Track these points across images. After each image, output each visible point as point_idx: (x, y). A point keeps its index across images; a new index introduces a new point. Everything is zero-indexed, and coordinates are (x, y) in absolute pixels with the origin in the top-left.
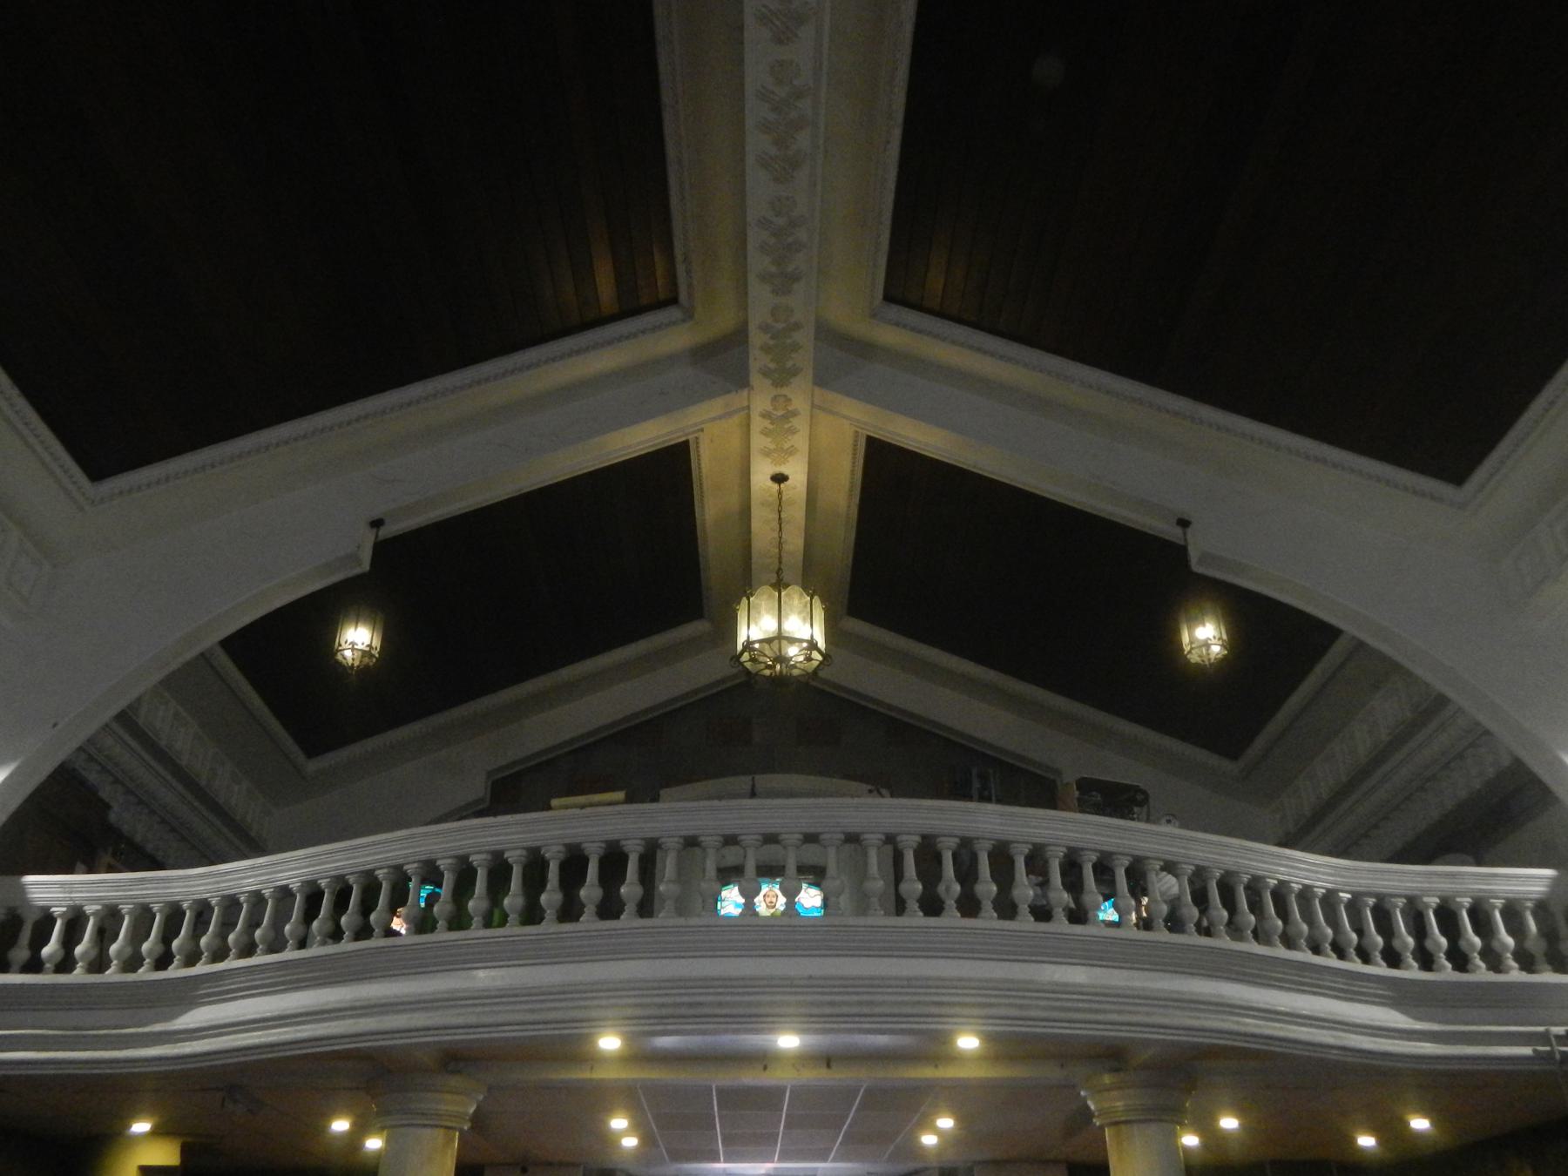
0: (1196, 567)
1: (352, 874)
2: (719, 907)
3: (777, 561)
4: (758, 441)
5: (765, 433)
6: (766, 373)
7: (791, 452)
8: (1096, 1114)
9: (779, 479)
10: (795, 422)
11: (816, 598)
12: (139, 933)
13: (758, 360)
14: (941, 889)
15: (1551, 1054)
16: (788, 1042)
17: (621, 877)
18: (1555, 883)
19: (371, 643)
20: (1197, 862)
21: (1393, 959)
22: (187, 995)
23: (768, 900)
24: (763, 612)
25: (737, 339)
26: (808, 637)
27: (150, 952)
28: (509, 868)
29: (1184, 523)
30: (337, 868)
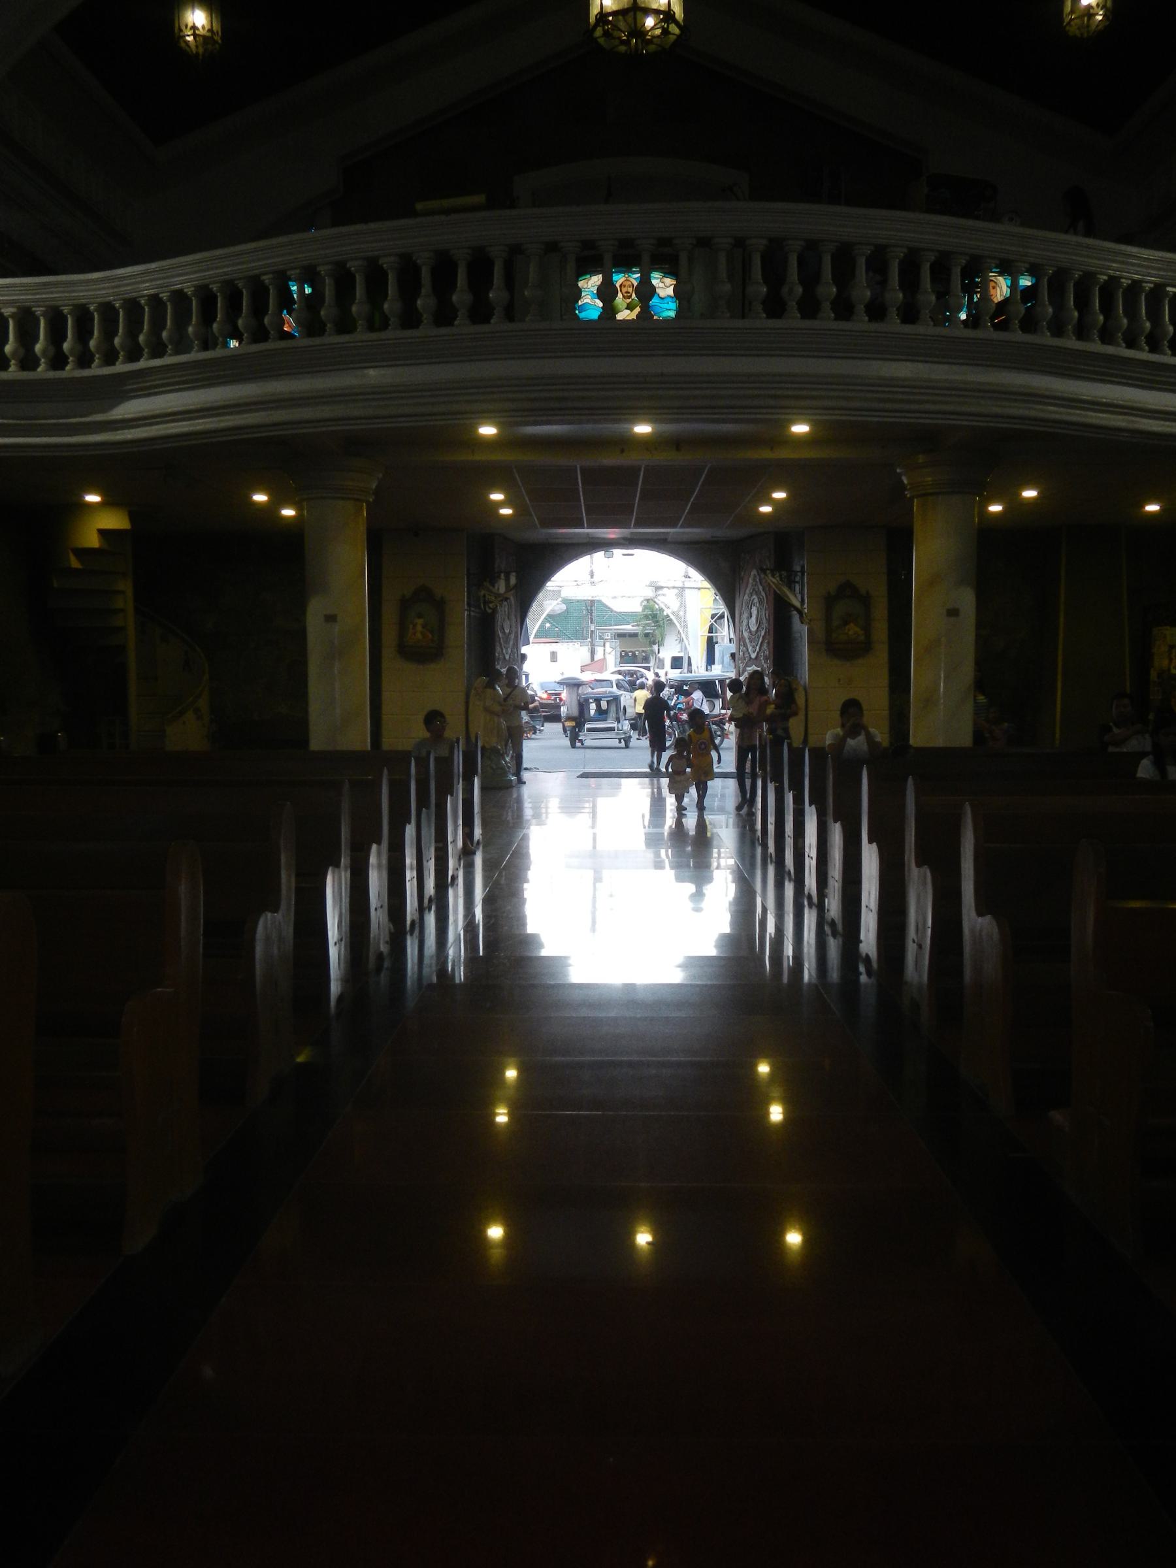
1: (240, 279)
8: (908, 487)
14: (785, 290)
16: (643, 429)
19: (212, 26)
20: (1032, 260)
22: (118, 389)
23: (624, 290)
27: (72, 350)
28: (384, 274)
30: (225, 274)
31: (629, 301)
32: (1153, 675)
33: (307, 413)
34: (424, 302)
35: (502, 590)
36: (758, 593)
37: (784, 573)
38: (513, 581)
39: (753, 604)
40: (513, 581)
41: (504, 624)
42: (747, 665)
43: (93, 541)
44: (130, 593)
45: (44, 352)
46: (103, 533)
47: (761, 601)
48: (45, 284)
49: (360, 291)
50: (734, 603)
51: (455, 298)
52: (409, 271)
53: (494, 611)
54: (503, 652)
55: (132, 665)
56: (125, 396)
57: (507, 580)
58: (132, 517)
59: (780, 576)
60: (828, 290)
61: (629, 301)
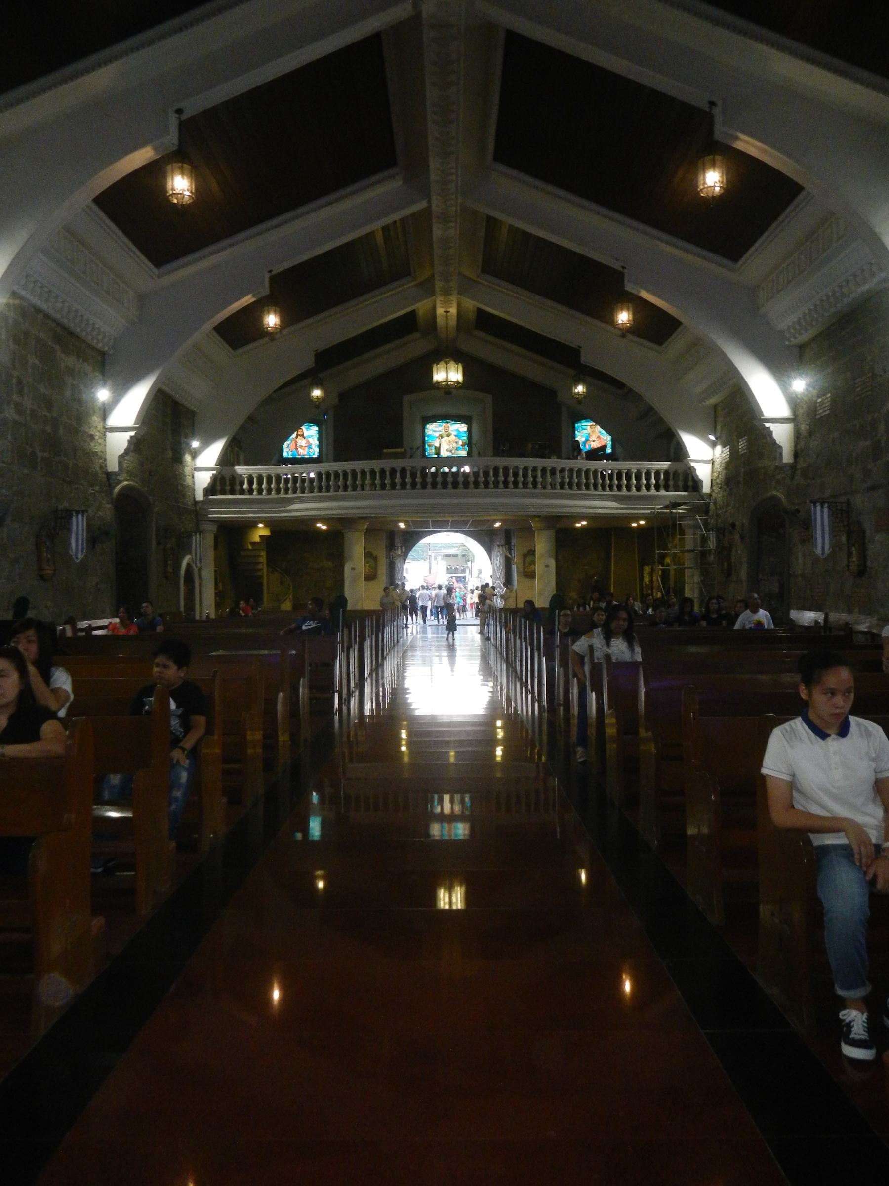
0: (582, 362)
3: (445, 319)
4: (438, 305)
6: (441, 295)
7: (451, 307)
9: (447, 312)
10: (452, 302)
11: (460, 364)
13: (437, 290)
15: (654, 513)
21: (619, 488)
22: (291, 501)
23: (445, 429)
24: (441, 371)
25: (431, 278)
26: (455, 380)
29: (580, 347)
31: (447, 433)
32: (644, 585)
35: (399, 553)
36: (499, 552)
37: (507, 546)
38: (404, 550)
39: (498, 556)
40: (404, 550)
41: (398, 564)
43: (257, 539)
44: (265, 557)
46: (260, 536)
47: (500, 555)
48: (267, 469)
49: (368, 477)
51: (396, 480)
52: (383, 472)
54: (398, 576)
55: (265, 584)
57: (401, 549)
58: (272, 531)
59: (505, 547)
60: (501, 478)
61: (447, 433)
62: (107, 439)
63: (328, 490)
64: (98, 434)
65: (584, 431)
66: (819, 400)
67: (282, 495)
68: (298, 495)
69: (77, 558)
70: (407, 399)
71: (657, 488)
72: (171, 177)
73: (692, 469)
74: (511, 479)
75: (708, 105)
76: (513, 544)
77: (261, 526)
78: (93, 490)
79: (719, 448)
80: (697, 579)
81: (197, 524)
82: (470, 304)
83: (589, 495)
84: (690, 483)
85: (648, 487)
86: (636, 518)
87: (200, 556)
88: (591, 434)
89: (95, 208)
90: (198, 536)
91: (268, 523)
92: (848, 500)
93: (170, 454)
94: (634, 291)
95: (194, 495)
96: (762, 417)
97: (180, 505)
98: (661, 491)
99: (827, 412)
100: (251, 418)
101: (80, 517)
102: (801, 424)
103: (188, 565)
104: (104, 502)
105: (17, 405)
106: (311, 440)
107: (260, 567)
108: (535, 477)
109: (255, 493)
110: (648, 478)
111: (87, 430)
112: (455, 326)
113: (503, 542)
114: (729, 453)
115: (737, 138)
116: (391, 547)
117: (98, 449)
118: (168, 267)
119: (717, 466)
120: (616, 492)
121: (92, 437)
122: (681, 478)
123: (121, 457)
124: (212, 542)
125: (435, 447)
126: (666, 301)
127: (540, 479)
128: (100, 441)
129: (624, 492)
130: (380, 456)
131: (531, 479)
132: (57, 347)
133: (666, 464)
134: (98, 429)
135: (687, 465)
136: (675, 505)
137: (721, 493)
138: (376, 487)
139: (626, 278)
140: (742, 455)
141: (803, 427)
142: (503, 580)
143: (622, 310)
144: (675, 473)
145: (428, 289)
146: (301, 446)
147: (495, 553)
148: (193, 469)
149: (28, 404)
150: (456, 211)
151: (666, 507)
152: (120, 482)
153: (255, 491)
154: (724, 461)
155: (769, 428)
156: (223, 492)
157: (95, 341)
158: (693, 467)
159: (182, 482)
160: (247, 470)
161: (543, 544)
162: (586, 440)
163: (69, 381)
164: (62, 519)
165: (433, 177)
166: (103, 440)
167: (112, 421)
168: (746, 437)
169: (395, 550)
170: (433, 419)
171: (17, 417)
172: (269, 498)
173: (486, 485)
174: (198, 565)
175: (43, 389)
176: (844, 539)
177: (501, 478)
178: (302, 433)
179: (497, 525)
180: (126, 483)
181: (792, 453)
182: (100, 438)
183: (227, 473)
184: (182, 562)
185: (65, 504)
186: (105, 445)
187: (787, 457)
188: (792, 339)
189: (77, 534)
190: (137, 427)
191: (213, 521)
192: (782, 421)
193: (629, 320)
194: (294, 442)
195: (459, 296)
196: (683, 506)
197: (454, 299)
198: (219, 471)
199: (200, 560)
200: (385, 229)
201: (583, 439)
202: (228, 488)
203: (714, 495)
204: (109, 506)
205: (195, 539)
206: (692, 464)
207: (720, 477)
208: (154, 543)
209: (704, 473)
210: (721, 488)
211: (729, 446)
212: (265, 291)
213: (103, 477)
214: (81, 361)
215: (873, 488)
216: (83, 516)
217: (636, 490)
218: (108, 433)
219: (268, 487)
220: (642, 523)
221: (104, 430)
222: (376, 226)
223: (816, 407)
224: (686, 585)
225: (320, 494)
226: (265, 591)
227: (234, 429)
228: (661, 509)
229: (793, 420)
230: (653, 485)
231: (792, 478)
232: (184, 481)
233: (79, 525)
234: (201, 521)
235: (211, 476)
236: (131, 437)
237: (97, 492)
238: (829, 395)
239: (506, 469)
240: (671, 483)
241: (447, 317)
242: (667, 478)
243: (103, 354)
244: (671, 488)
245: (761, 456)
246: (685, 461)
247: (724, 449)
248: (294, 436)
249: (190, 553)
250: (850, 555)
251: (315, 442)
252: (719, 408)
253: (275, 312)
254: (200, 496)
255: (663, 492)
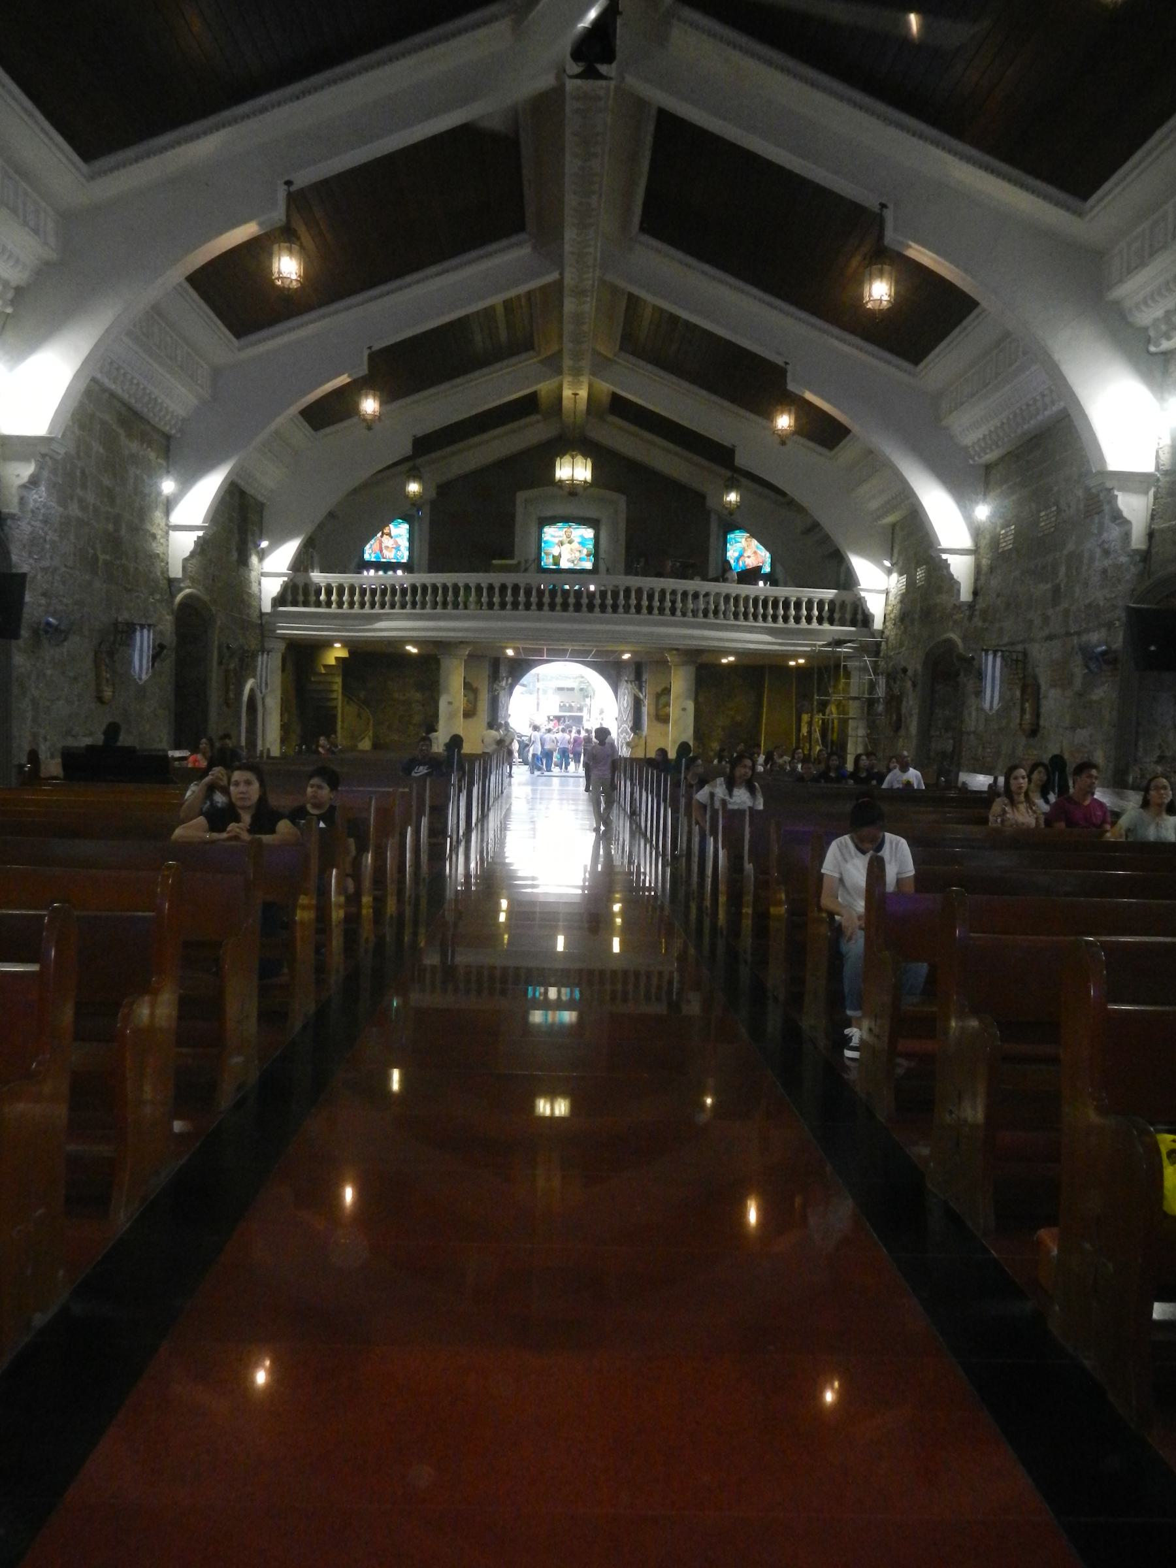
0: (736, 464)
2: (543, 536)
5: (569, 385)
6: (570, 374)
7: (581, 389)
9: (576, 394)
11: (589, 460)
12: (352, 594)
13: (565, 369)
17: (518, 595)
18: (836, 594)
21: (775, 618)
22: (378, 618)
26: (582, 479)
28: (482, 589)
29: (734, 446)
31: (569, 539)
33: (452, 634)
34: (496, 599)
36: (627, 689)
37: (637, 682)
40: (510, 681)
42: (622, 724)
43: (332, 662)
44: (340, 684)
45: (347, 600)
46: (337, 658)
47: (629, 693)
50: (617, 693)
53: (498, 694)
54: (501, 713)
56: (381, 620)
58: (350, 652)
60: (633, 601)
61: (569, 539)
62: (170, 539)
63: (423, 607)
64: (160, 532)
65: (738, 544)
66: (1003, 532)
67: (367, 610)
68: (387, 610)
69: (140, 679)
70: (521, 496)
71: (820, 620)
72: (277, 258)
73: (862, 600)
74: (645, 603)
75: (879, 207)
76: (644, 680)
77: (337, 645)
78: (153, 599)
79: (895, 576)
80: (861, 732)
81: (262, 642)
82: (605, 387)
83: (739, 626)
84: (860, 617)
85: (809, 619)
86: (795, 656)
87: (266, 678)
88: (746, 548)
89: (187, 285)
90: (265, 656)
91: (346, 643)
92: (1025, 649)
93: (235, 556)
94: (797, 392)
95: (260, 605)
96: (939, 547)
97: (245, 617)
98: (824, 625)
99: (1011, 546)
100: (331, 515)
101: (145, 632)
102: (983, 557)
103: (252, 690)
104: (164, 612)
105: (81, 501)
106: (399, 540)
107: (334, 696)
108: (673, 602)
109: (334, 605)
110: (809, 608)
111: (149, 527)
112: (585, 411)
113: (632, 677)
114: (905, 583)
115: (910, 247)
116: (495, 677)
117: (159, 550)
118: (253, 338)
119: (891, 597)
120: (770, 624)
121: (154, 536)
122: (849, 608)
123: (185, 560)
124: (279, 663)
125: (553, 557)
126: (835, 406)
127: (679, 605)
128: (162, 541)
129: (780, 624)
130: (487, 569)
131: (668, 604)
132: (121, 431)
133: (833, 592)
134: (161, 527)
135: (856, 595)
136: (839, 643)
137: (894, 630)
138: (482, 606)
139: (789, 374)
140: (919, 587)
141: (985, 562)
142: (631, 724)
143: (782, 413)
144: (843, 604)
145: (554, 365)
146: (387, 547)
147: (623, 690)
148: (260, 573)
149: (91, 498)
150: (593, 286)
151: (828, 645)
152: (181, 589)
153: (334, 603)
154: (899, 593)
155: (946, 560)
156: (295, 604)
157: (162, 423)
158: (864, 598)
159: (247, 590)
160: (325, 577)
161: (680, 683)
162: (739, 555)
163: (133, 471)
164: (124, 633)
165: (567, 248)
166: (165, 540)
167: (176, 518)
168: (924, 567)
169: (500, 682)
170: (552, 521)
171: (79, 514)
172: (350, 614)
173: (615, 608)
174: (263, 691)
175: (107, 482)
176: (1018, 693)
177: (633, 601)
178: (388, 531)
179: (626, 656)
180: (188, 591)
181: (971, 590)
182: (162, 537)
183: (300, 582)
184: (245, 686)
185: (124, 616)
186: (168, 546)
187: (965, 595)
188: (976, 458)
189: (141, 650)
190: (206, 526)
191: (283, 638)
192: (959, 552)
193: (789, 426)
194: (378, 541)
195: (591, 377)
196: (849, 644)
197: (585, 380)
198: (291, 577)
199: (266, 684)
200: (507, 304)
201: (736, 554)
202: (301, 598)
203: (887, 633)
204: (168, 617)
205: (261, 660)
206: (863, 594)
207: (895, 611)
208: (215, 663)
209: (876, 606)
210: (894, 624)
211: (905, 576)
212: (363, 370)
213: (163, 584)
214: (145, 446)
215: (1050, 638)
216: (149, 631)
217: (795, 622)
218: (171, 532)
219: (349, 599)
220: (801, 661)
221: (167, 528)
222: (496, 300)
223: (999, 540)
224: (850, 738)
225: (414, 611)
226: (339, 723)
227: (310, 528)
228: (823, 646)
229: (975, 552)
230: (815, 618)
231: (970, 618)
232: (250, 588)
233: (143, 641)
234: (269, 637)
235: (282, 583)
236: (199, 537)
237: (157, 600)
238: (1013, 527)
239: (639, 591)
240: (837, 616)
241: (575, 402)
242: (831, 611)
243: (168, 437)
244: (836, 623)
245: (939, 590)
246: (855, 589)
247: (900, 578)
248: (379, 535)
249: (254, 677)
250: (1023, 711)
251: (404, 543)
252: (897, 528)
253: (374, 397)
254: (267, 607)
255: (826, 626)
